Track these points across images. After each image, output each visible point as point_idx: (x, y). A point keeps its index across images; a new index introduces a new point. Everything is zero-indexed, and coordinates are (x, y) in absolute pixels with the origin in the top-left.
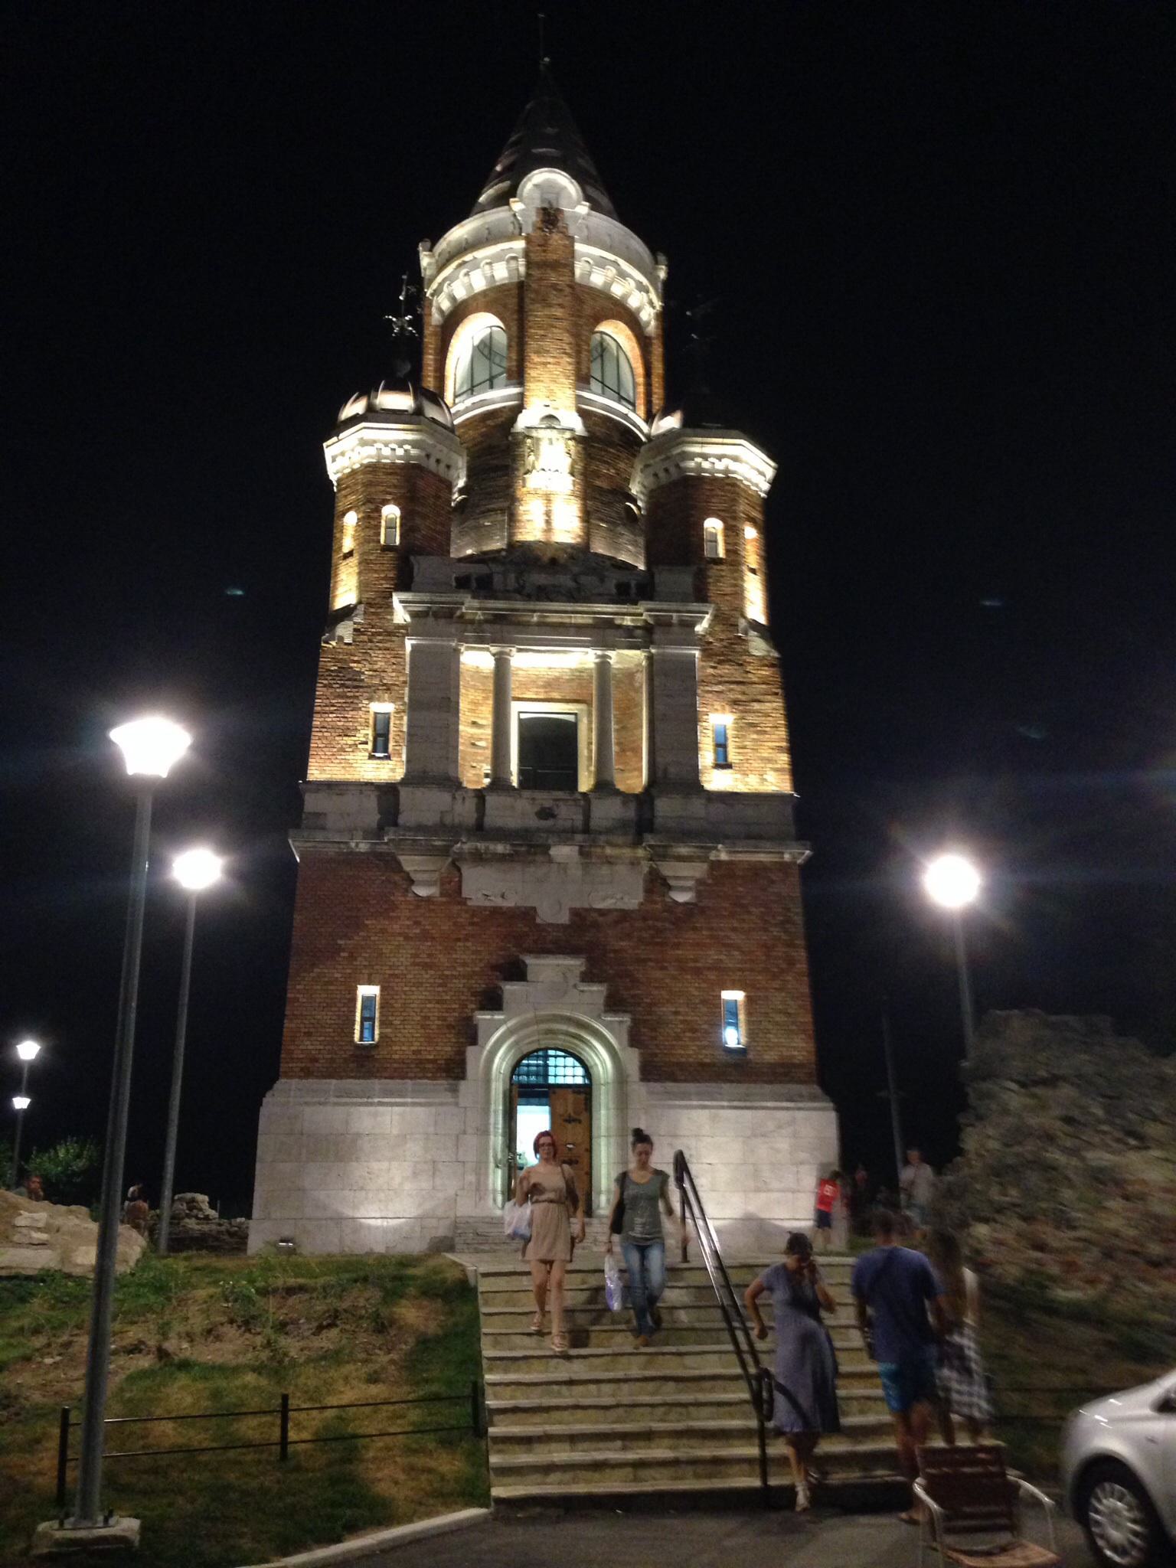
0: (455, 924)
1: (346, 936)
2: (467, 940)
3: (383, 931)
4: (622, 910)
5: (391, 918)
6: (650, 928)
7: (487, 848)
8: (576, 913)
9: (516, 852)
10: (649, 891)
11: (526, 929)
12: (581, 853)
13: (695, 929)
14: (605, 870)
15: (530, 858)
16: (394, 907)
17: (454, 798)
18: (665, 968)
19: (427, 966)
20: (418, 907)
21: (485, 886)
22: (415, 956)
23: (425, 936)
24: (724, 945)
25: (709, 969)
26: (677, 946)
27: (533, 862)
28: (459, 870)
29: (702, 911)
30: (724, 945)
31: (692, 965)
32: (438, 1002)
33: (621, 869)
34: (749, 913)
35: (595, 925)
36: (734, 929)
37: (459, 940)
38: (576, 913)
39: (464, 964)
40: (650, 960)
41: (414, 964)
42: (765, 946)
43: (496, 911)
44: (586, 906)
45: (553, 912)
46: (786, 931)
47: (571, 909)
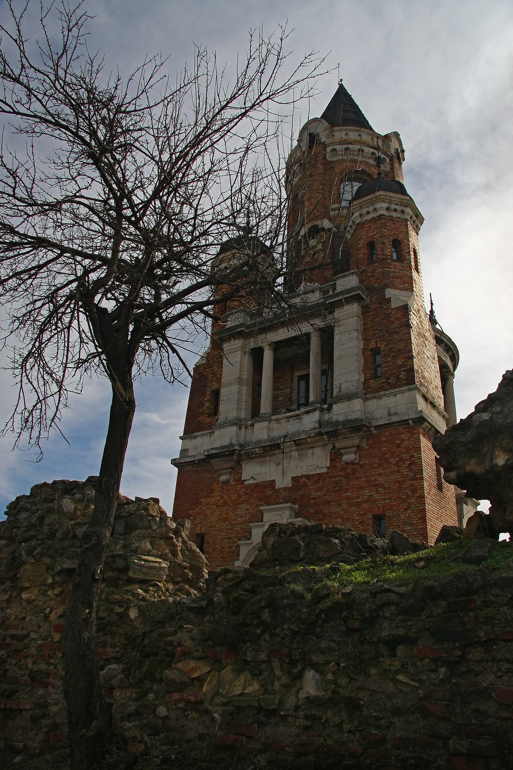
0: (238, 495)
1: (194, 509)
2: (243, 503)
3: (208, 504)
4: (319, 474)
5: (212, 497)
6: (333, 482)
7: (252, 452)
8: (295, 479)
9: (266, 451)
10: (332, 460)
11: (271, 493)
12: (296, 445)
13: (358, 478)
14: (310, 452)
15: (273, 452)
16: (213, 490)
17: (240, 428)
18: (341, 505)
19: (225, 520)
20: (223, 489)
21: (253, 472)
22: (221, 515)
23: (225, 504)
24: (375, 485)
25: (365, 502)
26: (347, 490)
27: (275, 454)
28: (241, 465)
29: (362, 466)
30: (375, 485)
31: (356, 500)
32: (229, 538)
33: (318, 451)
34: (389, 463)
35: (305, 485)
36: (380, 475)
37: (239, 504)
38: (295, 479)
39: (241, 517)
40: (332, 501)
41: (220, 519)
42: (398, 482)
43: (257, 485)
44: (300, 475)
45: (283, 482)
46: (410, 470)
47: (292, 478)
